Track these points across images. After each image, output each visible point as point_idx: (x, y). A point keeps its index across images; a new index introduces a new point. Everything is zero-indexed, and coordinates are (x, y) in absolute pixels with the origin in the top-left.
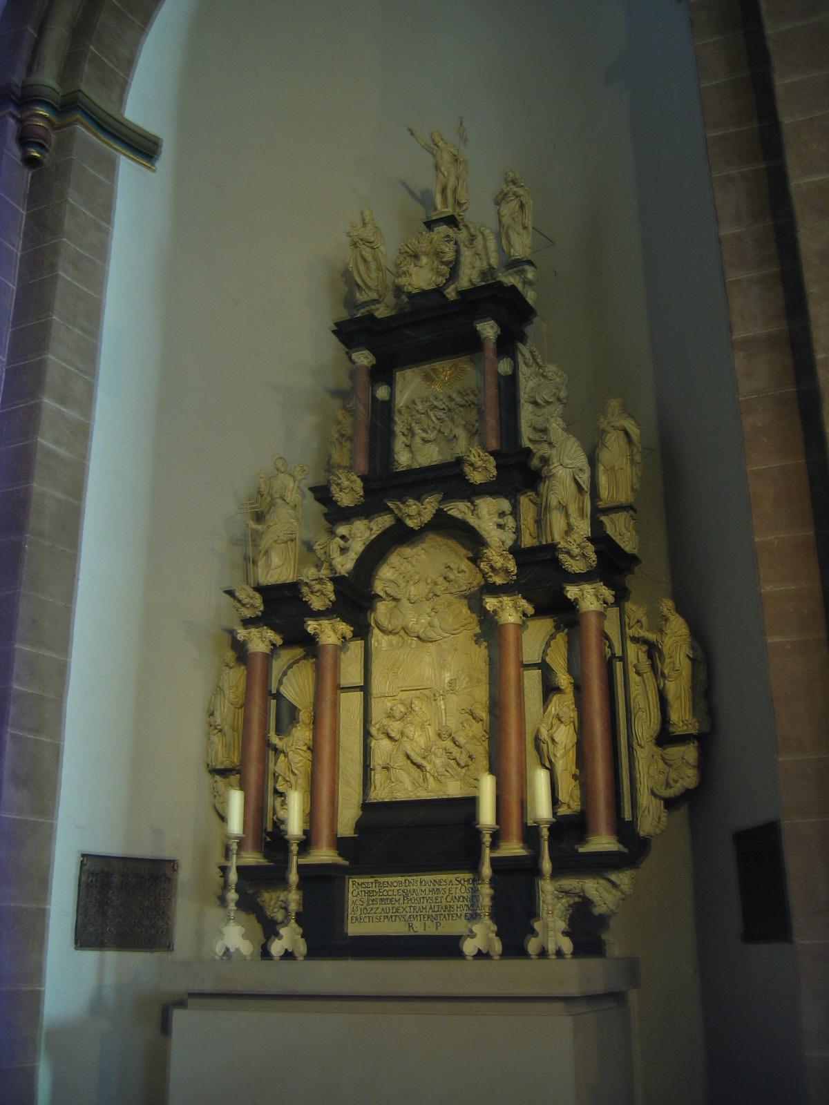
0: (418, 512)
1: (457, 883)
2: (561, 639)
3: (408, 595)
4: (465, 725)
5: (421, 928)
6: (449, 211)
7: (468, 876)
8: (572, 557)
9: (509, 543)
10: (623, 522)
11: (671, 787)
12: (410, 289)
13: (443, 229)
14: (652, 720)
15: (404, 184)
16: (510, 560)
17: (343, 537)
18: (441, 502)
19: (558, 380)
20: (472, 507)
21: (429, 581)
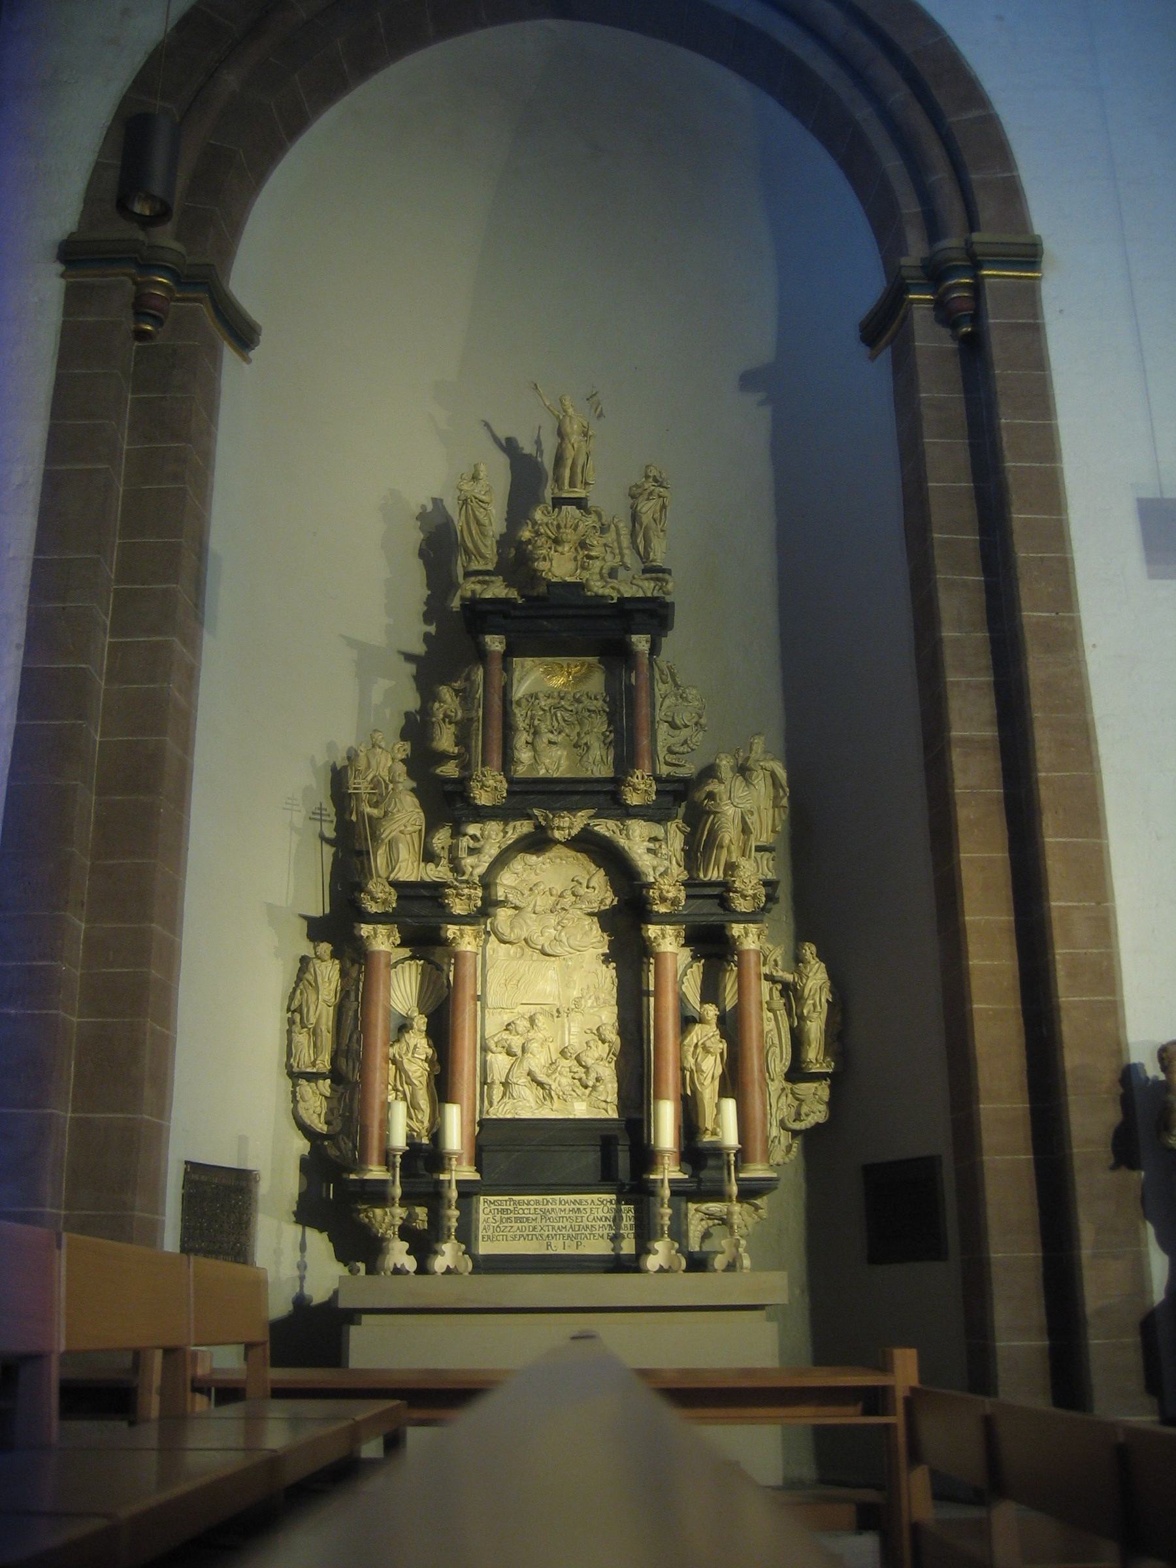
0: (569, 824)
1: (599, 1203)
2: (697, 970)
3: (533, 902)
4: (592, 1044)
5: (559, 1248)
6: (579, 492)
7: (614, 1197)
8: (744, 897)
9: (662, 869)
10: (765, 862)
11: (802, 1121)
12: (550, 576)
13: (571, 510)
14: (784, 1057)
15: (487, 425)
16: (680, 890)
17: (474, 837)
18: (590, 817)
19: (697, 703)
20: (622, 827)
21: (554, 892)
